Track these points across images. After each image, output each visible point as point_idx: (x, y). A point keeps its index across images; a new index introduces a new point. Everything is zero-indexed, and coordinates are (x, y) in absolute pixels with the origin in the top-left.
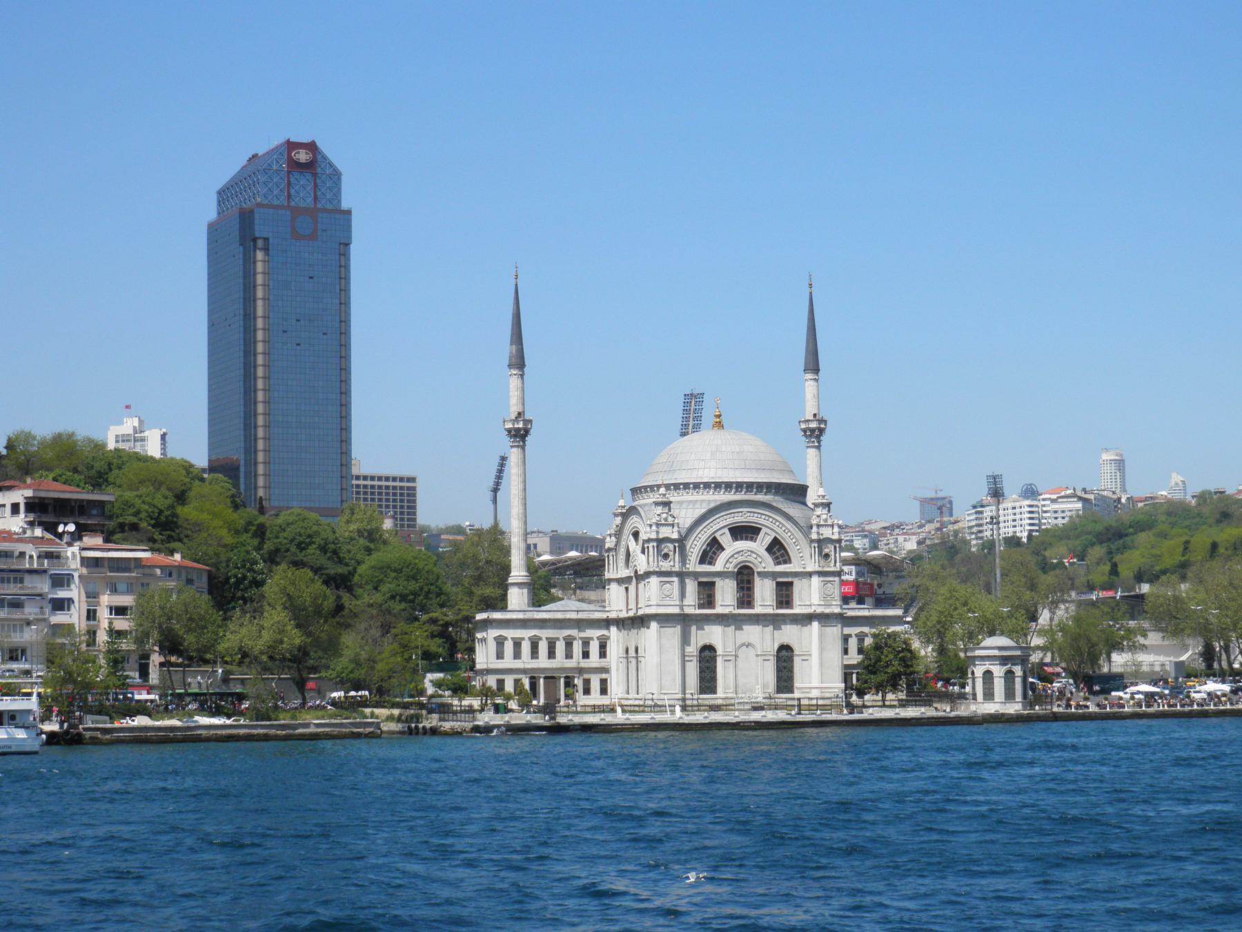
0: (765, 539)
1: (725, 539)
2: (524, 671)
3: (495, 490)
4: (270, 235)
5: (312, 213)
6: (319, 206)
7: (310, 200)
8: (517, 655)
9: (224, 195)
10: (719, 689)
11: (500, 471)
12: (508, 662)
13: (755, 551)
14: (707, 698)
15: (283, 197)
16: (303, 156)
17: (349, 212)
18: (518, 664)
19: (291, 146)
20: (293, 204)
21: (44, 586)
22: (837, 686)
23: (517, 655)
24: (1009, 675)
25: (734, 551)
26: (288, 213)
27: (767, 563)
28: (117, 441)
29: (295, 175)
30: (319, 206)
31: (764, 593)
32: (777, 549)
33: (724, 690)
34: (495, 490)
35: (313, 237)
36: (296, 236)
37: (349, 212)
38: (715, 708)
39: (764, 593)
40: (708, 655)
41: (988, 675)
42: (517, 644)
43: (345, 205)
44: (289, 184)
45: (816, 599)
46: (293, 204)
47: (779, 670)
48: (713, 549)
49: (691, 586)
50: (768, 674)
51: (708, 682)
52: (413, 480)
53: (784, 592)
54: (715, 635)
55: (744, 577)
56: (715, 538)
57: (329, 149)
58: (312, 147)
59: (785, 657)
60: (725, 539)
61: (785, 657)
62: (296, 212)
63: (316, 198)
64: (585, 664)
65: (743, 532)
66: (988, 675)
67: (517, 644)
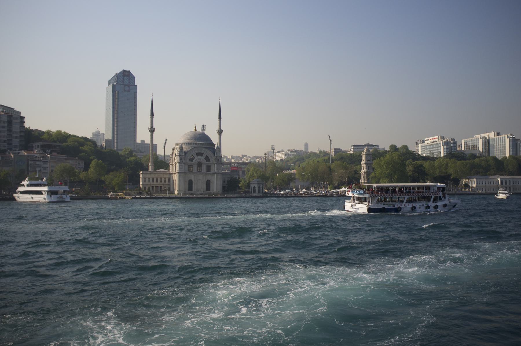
0: (204, 156)
3: (164, 146)
8: (149, 181)
9: (110, 82)
11: (166, 142)
13: (202, 159)
14: (190, 192)
16: (127, 74)
18: (149, 183)
19: (124, 71)
21: (41, 163)
22: (220, 190)
23: (149, 181)
24: (259, 187)
25: (197, 158)
31: (204, 168)
33: (194, 190)
34: (164, 146)
35: (129, 91)
36: (125, 91)
38: (192, 194)
39: (204, 168)
40: (190, 182)
41: (254, 187)
42: (149, 179)
44: (123, 79)
45: (215, 169)
47: (207, 186)
49: (187, 167)
50: (205, 186)
51: (190, 188)
53: (209, 168)
55: (200, 165)
58: (129, 72)
59: (208, 183)
61: (208, 183)
62: (125, 85)
63: (129, 82)
64: (164, 183)
65: (199, 154)
66: (254, 187)
67: (149, 179)
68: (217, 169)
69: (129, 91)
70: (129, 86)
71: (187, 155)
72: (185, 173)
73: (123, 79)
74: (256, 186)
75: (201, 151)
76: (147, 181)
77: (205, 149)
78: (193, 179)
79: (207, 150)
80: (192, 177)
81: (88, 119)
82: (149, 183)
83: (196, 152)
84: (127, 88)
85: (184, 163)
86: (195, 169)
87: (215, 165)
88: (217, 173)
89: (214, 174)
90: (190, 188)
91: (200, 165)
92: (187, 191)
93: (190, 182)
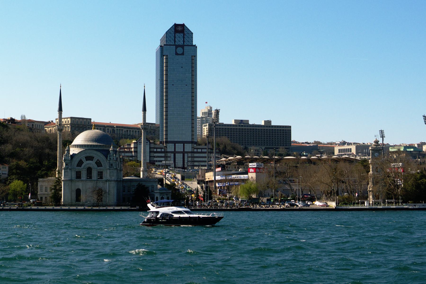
1: (84, 160)
2: (48, 194)
4: (168, 54)
5: (182, 46)
6: (185, 44)
7: (182, 42)
10: (81, 201)
12: (44, 192)
13: (92, 164)
15: (173, 42)
16: (180, 28)
17: (195, 45)
18: (46, 193)
19: (176, 25)
20: (176, 44)
25: (87, 163)
26: (175, 47)
27: (96, 166)
28: (203, 114)
29: (177, 35)
30: (185, 44)
32: (99, 164)
35: (183, 54)
36: (177, 54)
37: (195, 45)
39: (95, 174)
40: (78, 192)
41: (157, 197)
43: (194, 44)
44: (175, 37)
46: (176, 44)
48: (80, 163)
51: (78, 198)
52: (290, 127)
53: (100, 175)
54: (80, 185)
55: (89, 170)
56: (81, 160)
57: (189, 26)
58: (183, 25)
60: (84, 160)
62: (177, 46)
63: (184, 41)
68: (110, 176)
69: (183, 54)
70: (182, 46)
71: (74, 159)
72: (71, 180)
73: (175, 37)
74: (158, 196)
75: (91, 155)
76: (44, 190)
77: (95, 152)
78: (81, 188)
79: (99, 154)
80: (80, 185)
81: (124, 97)
82: (46, 193)
83: (86, 155)
84: (180, 50)
85: (70, 169)
86: (84, 175)
87: (108, 171)
88: (109, 181)
89: (107, 181)
90: (78, 198)
91: (89, 170)
92: (74, 202)
93: (78, 192)
